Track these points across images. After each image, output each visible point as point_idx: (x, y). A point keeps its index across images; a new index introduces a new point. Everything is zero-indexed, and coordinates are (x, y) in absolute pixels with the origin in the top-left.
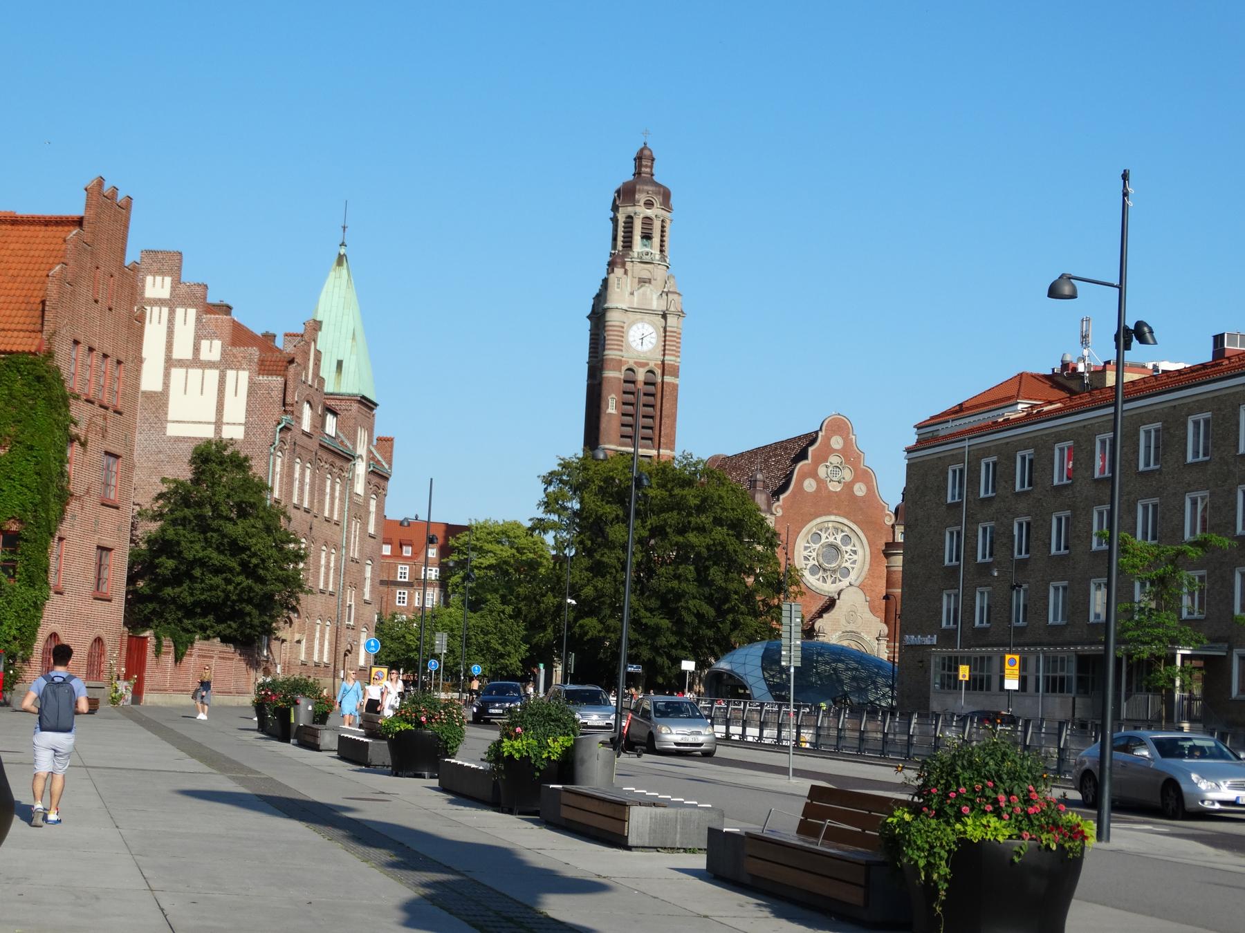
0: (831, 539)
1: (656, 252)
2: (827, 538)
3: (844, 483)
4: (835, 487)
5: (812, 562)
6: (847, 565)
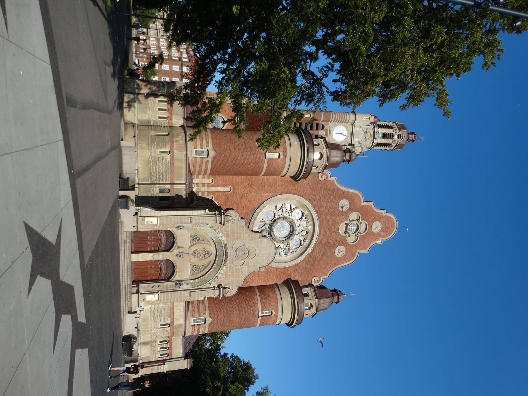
0: (298, 230)
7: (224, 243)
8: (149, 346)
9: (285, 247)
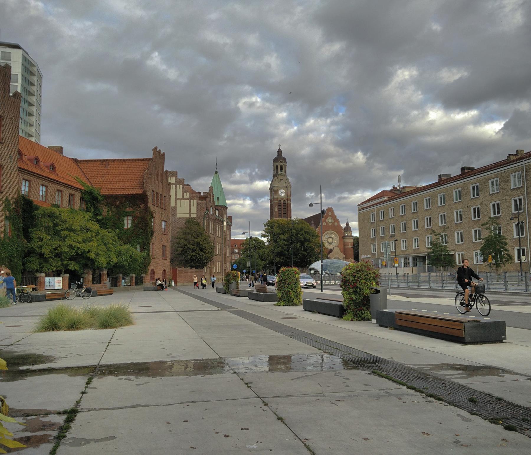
0: (330, 236)
1: (284, 173)
4: (330, 224)
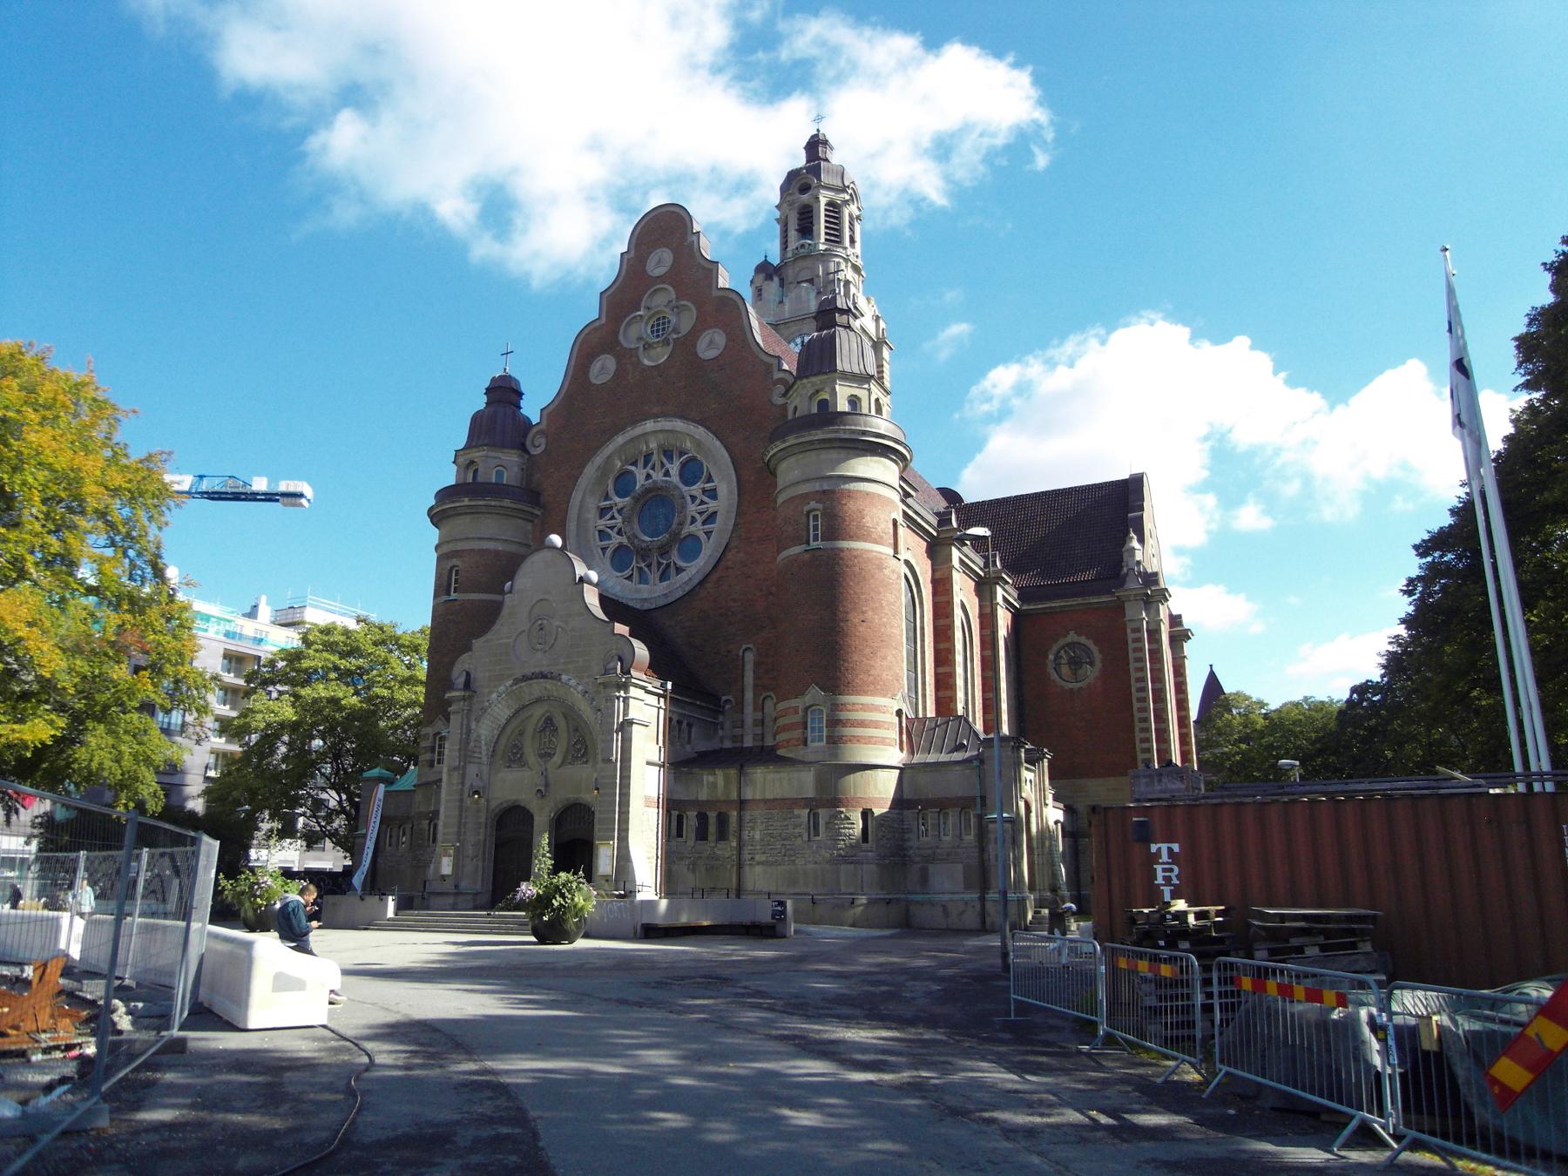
0: (658, 476)
2: (648, 476)
3: (676, 340)
5: (616, 540)
6: (697, 529)
7: (511, 686)
8: (931, 868)
9: (698, 501)
